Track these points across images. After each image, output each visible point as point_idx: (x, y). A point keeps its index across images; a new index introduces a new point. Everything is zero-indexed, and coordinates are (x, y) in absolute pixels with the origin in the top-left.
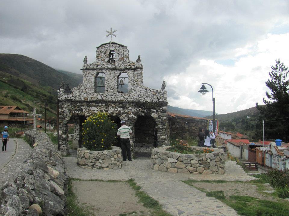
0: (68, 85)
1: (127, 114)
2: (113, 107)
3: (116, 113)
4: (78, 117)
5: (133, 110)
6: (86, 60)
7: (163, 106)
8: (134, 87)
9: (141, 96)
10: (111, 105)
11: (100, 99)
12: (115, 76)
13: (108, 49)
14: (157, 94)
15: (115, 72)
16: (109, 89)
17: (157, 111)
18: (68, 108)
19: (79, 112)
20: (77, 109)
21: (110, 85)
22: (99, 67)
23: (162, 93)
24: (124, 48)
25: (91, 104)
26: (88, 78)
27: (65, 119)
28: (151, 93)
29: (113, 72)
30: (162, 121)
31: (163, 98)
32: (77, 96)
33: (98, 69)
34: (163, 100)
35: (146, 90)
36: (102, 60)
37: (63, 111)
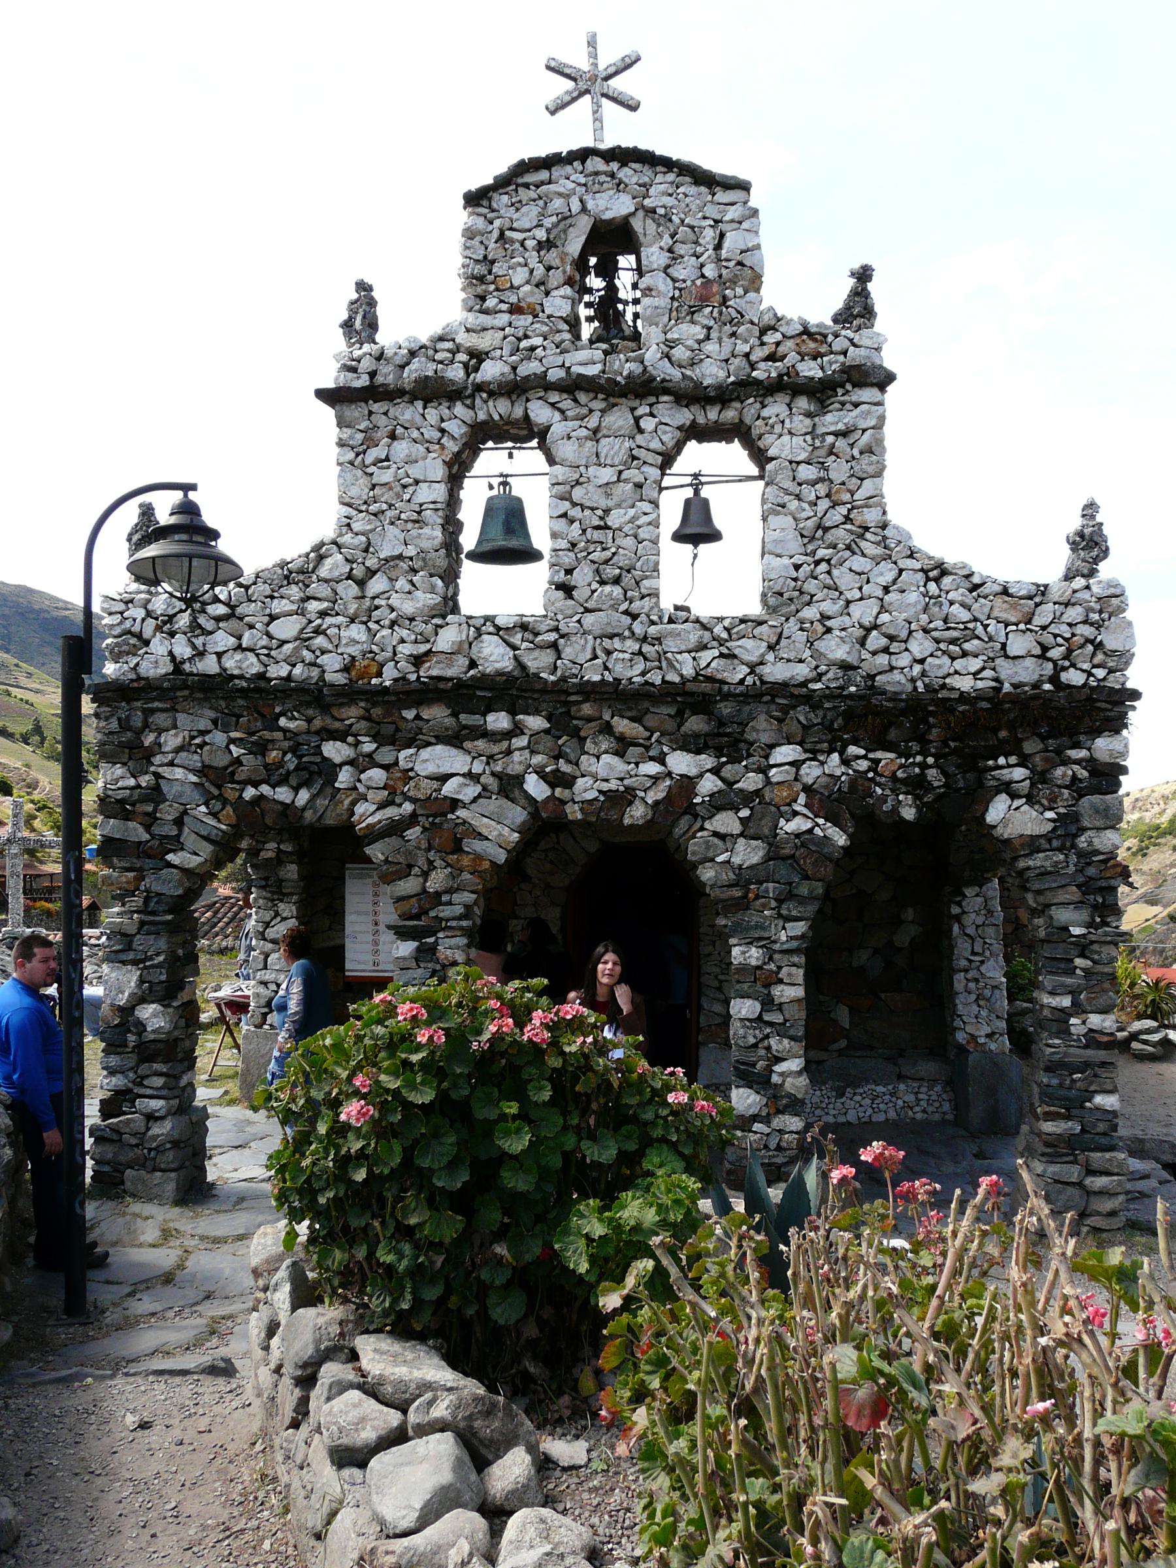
0: (187, 488)
1: (760, 811)
2: (623, 745)
3: (651, 798)
4: (287, 847)
5: (811, 772)
6: (362, 318)
7: (1098, 733)
8: (821, 553)
9: (892, 638)
10: (607, 729)
11: (500, 673)
12: (642, 453)
13: (576, 206)
14: (1038, 621)
15: (637, 420)
16: (583, 576)
17: (1040, 777)
18: (195, 760)
19: (296, 790)
20: (281, 764)
21: (597, 535)
22: (491, 371)
23: (1090, 610)
24: (722, 196)
25: (409, 714)
26: (386, 476)
27: (170, 857)
28: (981, 608)
29: (619, 419)
30: (1091, 871)
31: (1100, 657)
32: (285, 642)
33: (479, 388)
34: (1100, 673)
35: (937, 580)
36: (515, 310)
37: (145, 780)
